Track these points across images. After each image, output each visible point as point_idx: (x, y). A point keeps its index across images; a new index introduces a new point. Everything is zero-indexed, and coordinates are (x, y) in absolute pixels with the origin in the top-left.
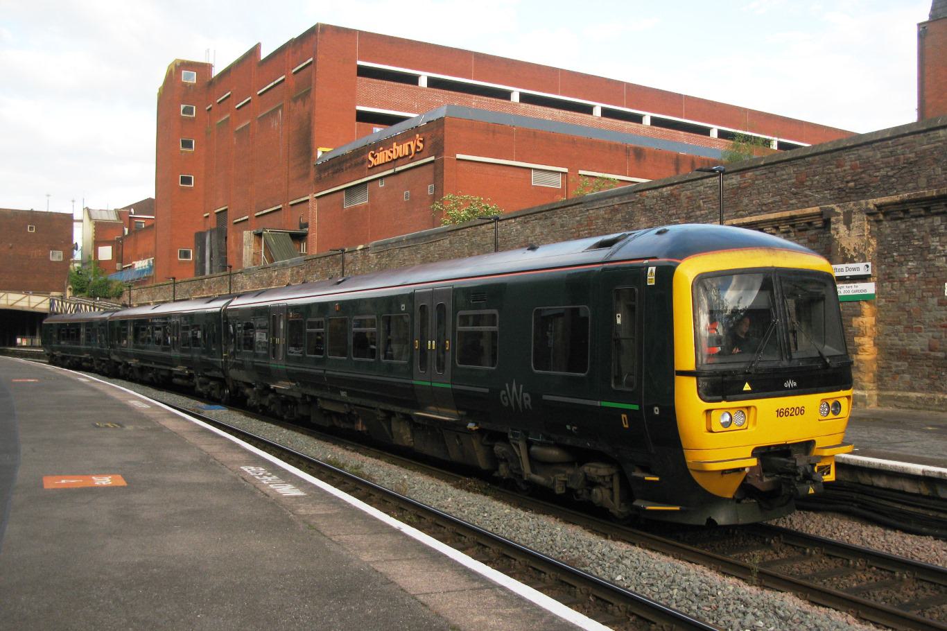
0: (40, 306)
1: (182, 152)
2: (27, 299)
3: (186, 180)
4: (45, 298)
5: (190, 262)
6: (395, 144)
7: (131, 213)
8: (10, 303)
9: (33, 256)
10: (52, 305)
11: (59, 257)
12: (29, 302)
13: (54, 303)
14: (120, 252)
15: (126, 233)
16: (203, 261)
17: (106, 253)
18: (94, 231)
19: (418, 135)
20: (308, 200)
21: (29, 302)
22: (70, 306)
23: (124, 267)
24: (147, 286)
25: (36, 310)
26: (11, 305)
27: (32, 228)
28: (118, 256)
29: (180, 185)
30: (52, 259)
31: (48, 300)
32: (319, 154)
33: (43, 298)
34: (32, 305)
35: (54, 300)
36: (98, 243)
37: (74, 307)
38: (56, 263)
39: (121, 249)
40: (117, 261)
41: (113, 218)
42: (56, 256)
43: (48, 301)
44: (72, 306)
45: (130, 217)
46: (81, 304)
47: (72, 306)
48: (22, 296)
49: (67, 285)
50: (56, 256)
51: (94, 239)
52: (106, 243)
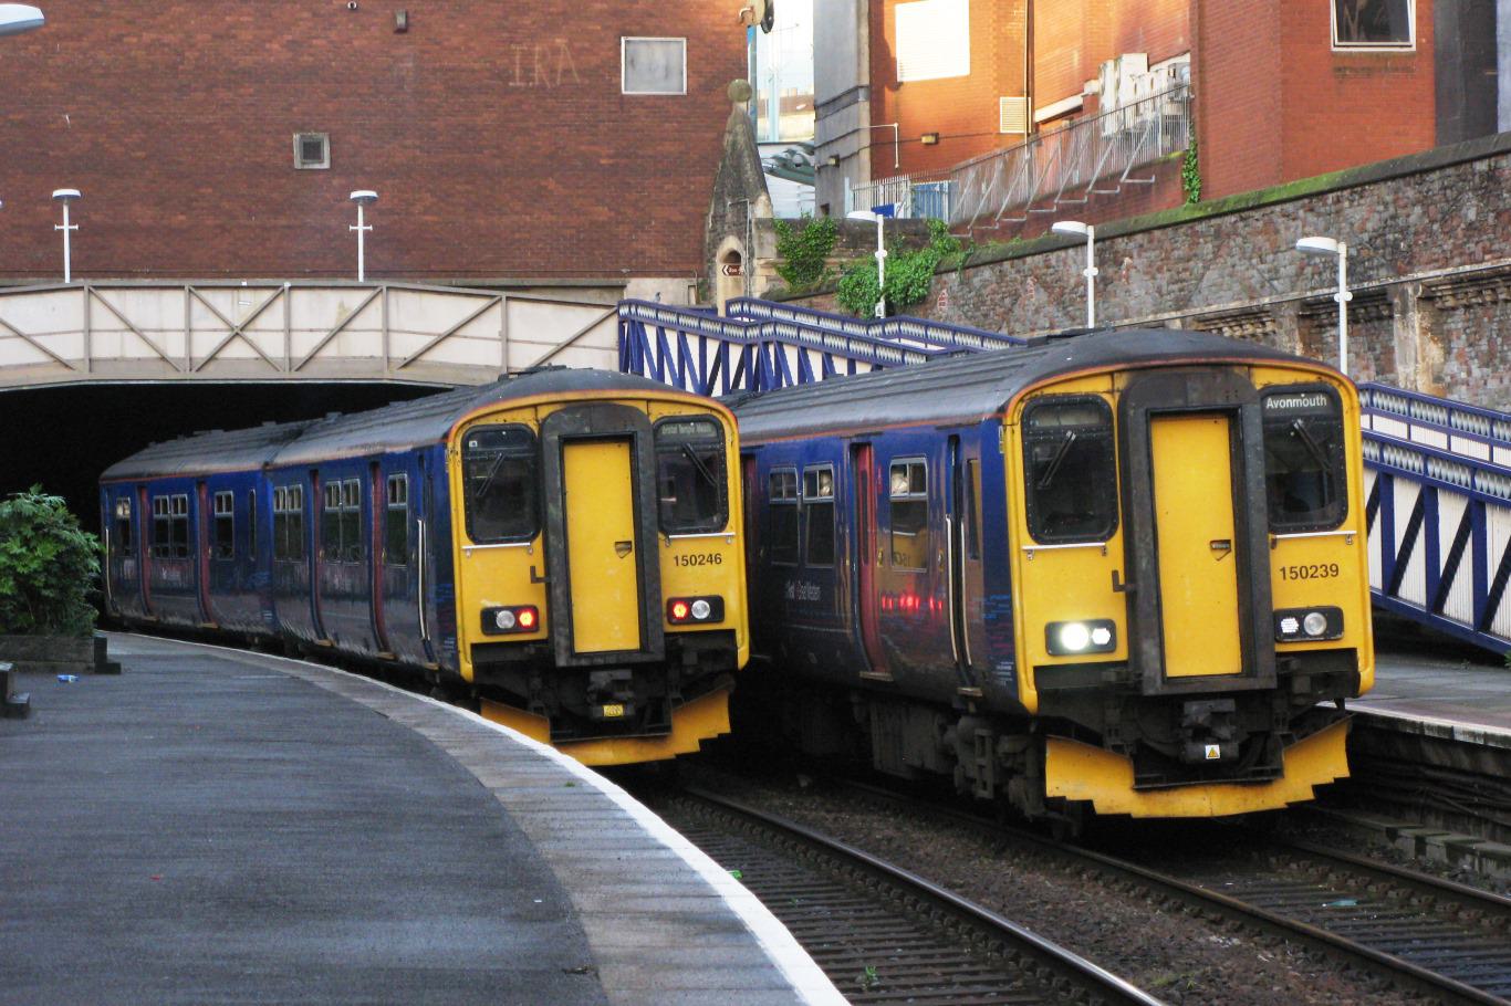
2: (491, 324)
4: (600, 313)
5: (1402, 64)
8: (404, 347)
9: (527, 77)
10: (631, 349)
13: (642, 345)
22: (722, 357)
23: (1040, 116)
24: (1147, 219)
26: (407, 364)
30: (633, 85)
31: (613, 323)
33: (579, 318)
35: (638, 326)
37: (744, 362)
38: (655, 106)
43: (609, 333)
44: (735, 353)
46: (780, 345)
47: (735, 353)
48: (472, 305)
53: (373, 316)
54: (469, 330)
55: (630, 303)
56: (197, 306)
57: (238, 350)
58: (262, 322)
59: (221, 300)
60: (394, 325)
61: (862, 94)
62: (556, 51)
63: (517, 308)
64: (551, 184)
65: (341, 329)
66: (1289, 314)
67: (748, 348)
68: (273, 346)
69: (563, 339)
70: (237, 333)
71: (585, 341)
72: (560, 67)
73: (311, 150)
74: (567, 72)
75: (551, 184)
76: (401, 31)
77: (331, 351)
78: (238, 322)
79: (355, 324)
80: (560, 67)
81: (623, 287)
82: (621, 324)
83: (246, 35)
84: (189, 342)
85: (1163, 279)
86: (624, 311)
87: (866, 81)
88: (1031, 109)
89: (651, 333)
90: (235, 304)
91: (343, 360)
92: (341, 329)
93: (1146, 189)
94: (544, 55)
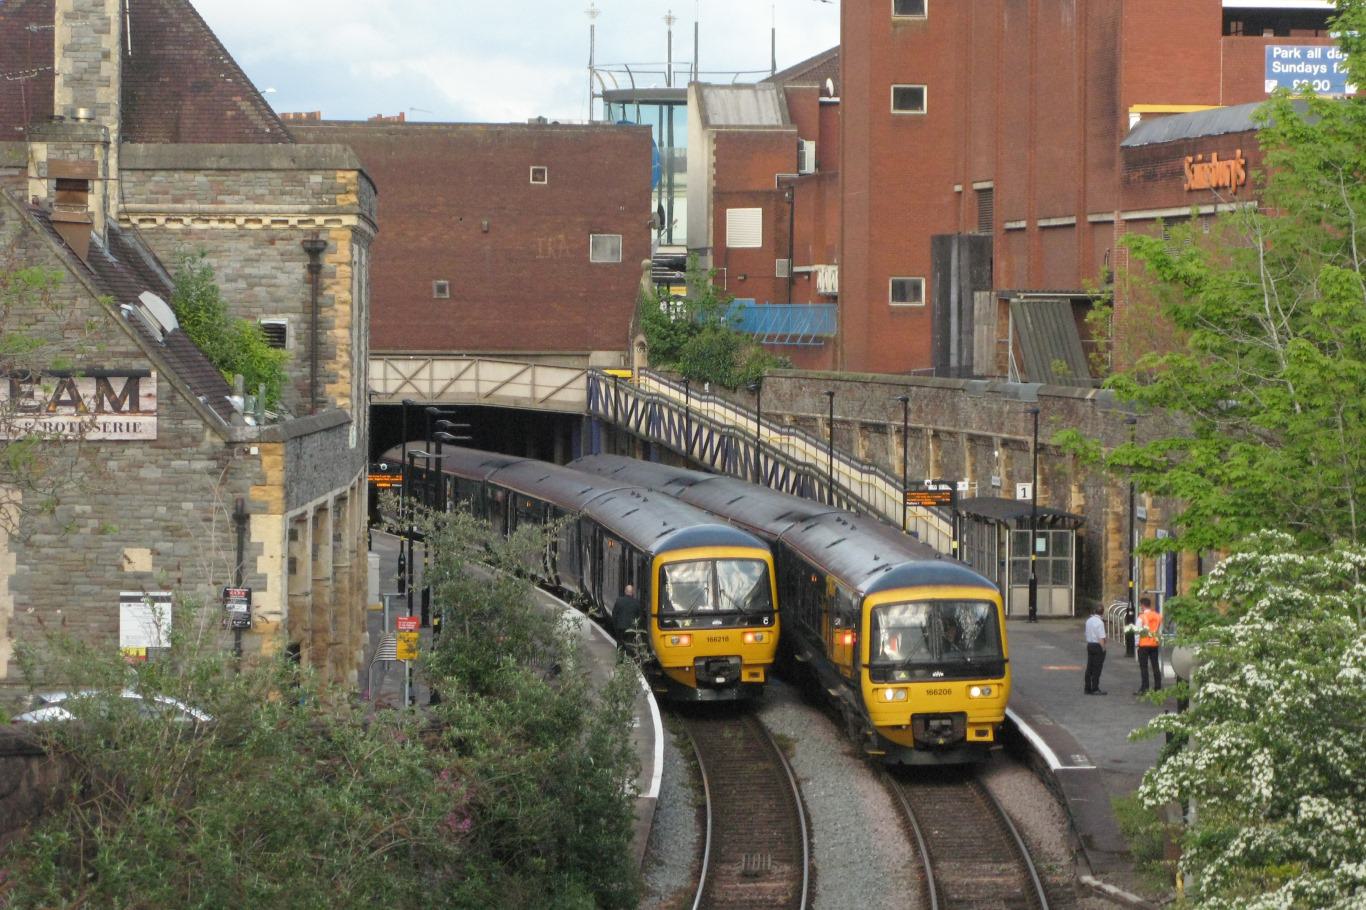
0: (561, 396)
1: (896, 25)
2: (526, 377)
3: (909, 98)
4: (578, 373)
5: (919, 311)
6: (1214, 155)
7: (825, 92)
8: (485, 388)
10: (592, 393)
11: (614, 252)
12: (533, 384)
13: (598, 390)
14: (786, 226)
15: (810, 166)
16: (946, 315)
17: (746, 227)
18: (714, 159)
19: (1239, 152)
20: (1112, 222)
21: (533, 384)
22: (635, 404)
23: (797, 269)
24: (812, 373)
25: (552, 407)
26: (488, 395)
27: (542, 171)
28: (781, 237)
29: (894, 112)
30: (595, 258)
31: (584, 377)
32: (1134, 120)
33: (567, 375)
34: (542, 393)
35: (596, 380)
36: (725, 196)
38: (605, 267)
39: (787, 217)
40: (779, 254)
41: (764, 113)
42: (606, 250)
43: (582, 382)
44: (641, 406)
45: (822, 104)
46: (661, 405)
47: (641, 406)
48: (517, 369)
49: (633, 337)
50: (606, 250)
51: (714, 184)
52: (747, 199)
53: (471, 374)
54: (517, 380)
55: (592, 369)
56: (390, 368)
57: (408, 389)
58: (422, 375)
59: (401, 365)
60: (482, 377)
61: (709, 252)
62: (559, 241)
63: (539, 371)
64: (555, 305)
65: (456, 379)
66: (857, 428)
67: (647, 404)
68: (425, 387)
69: (560, 384)
70: (407, 381)
71: (571, 386)
72: (561, 247)
73: (441, 289)
74: (564, 251)
75: (555, 305)
76: (486, 232)
77: (451, 389)
78: (407, 376)
79: (463, 377)
80: (561, 247)
81: (588, 355)
82: (588, 378)
83: (411, 234)
84: (385, 385)
85: (817, 400)
86: (590, 372)
87: (711, 244)
88: (791, 266)
89: (603, 387)
90: (406, 367)
91: (458, 394)
92: (456, 379)
93: (821, 347)
94: (552, 243)
